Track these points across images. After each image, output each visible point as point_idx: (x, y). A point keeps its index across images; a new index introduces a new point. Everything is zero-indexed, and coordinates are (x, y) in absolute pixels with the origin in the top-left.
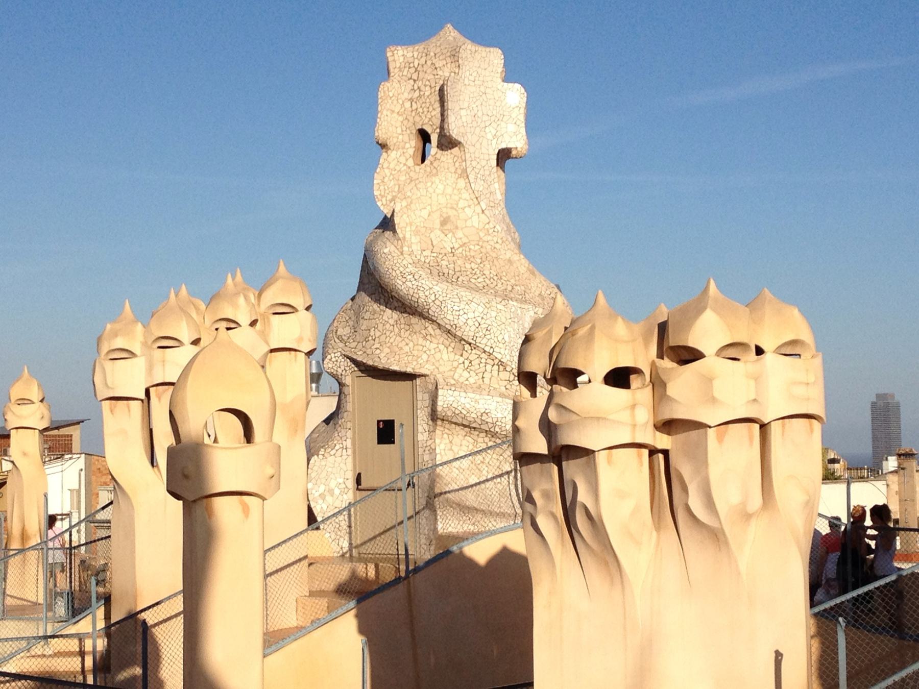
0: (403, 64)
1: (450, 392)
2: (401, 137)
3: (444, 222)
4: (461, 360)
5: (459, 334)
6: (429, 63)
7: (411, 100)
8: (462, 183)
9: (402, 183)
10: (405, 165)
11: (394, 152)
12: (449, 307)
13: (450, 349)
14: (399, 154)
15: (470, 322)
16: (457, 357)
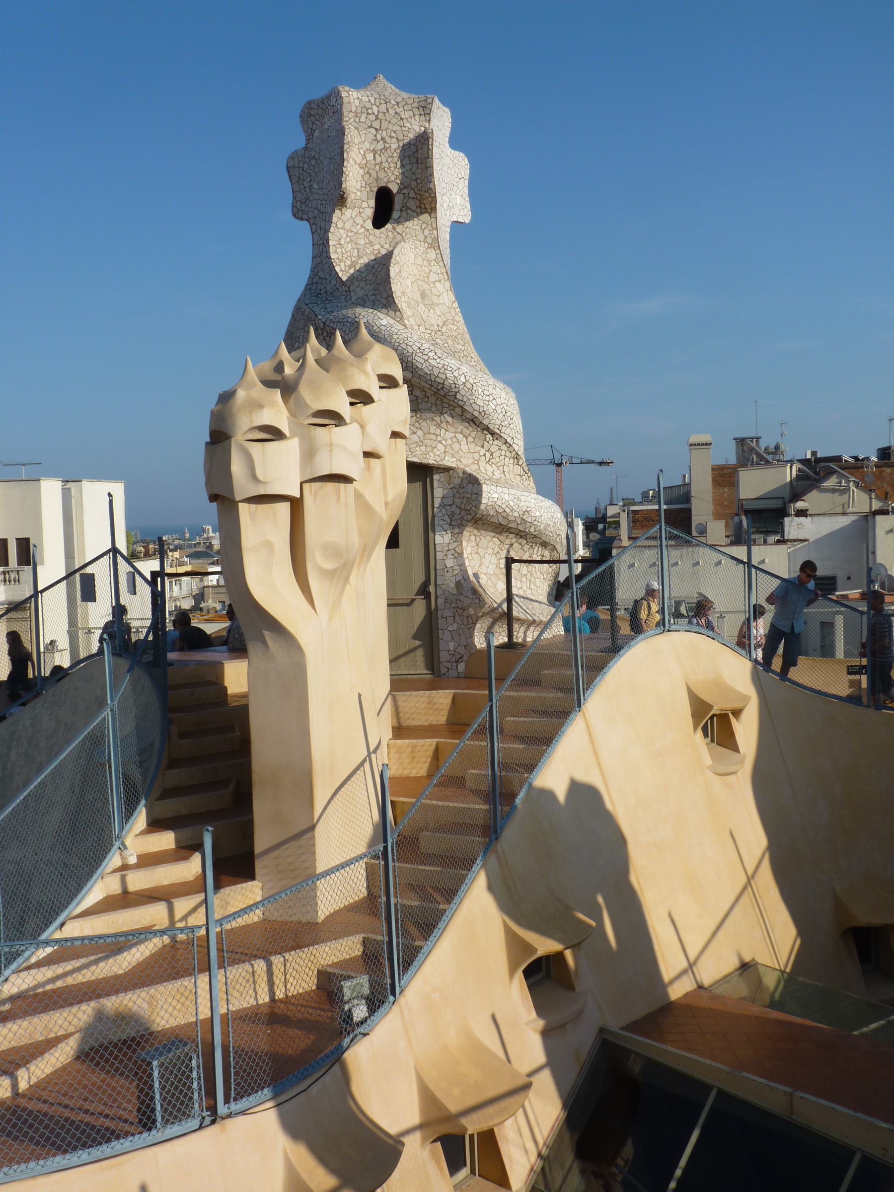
0: (359, 110)
1: (494, 488)
2: (359, 193)
3: (423, 296)
4: (483, 451)
5: (486, 422)
6: (392, 112)
7: (375, 152)
8: (432, 254)
9: (361, 247)
10: (362, 226)
11: (350, 210)
12: (480, 390)
13: (470, 439)
14: (354, 213)
15: (498, 409)
16: (478, 448)
